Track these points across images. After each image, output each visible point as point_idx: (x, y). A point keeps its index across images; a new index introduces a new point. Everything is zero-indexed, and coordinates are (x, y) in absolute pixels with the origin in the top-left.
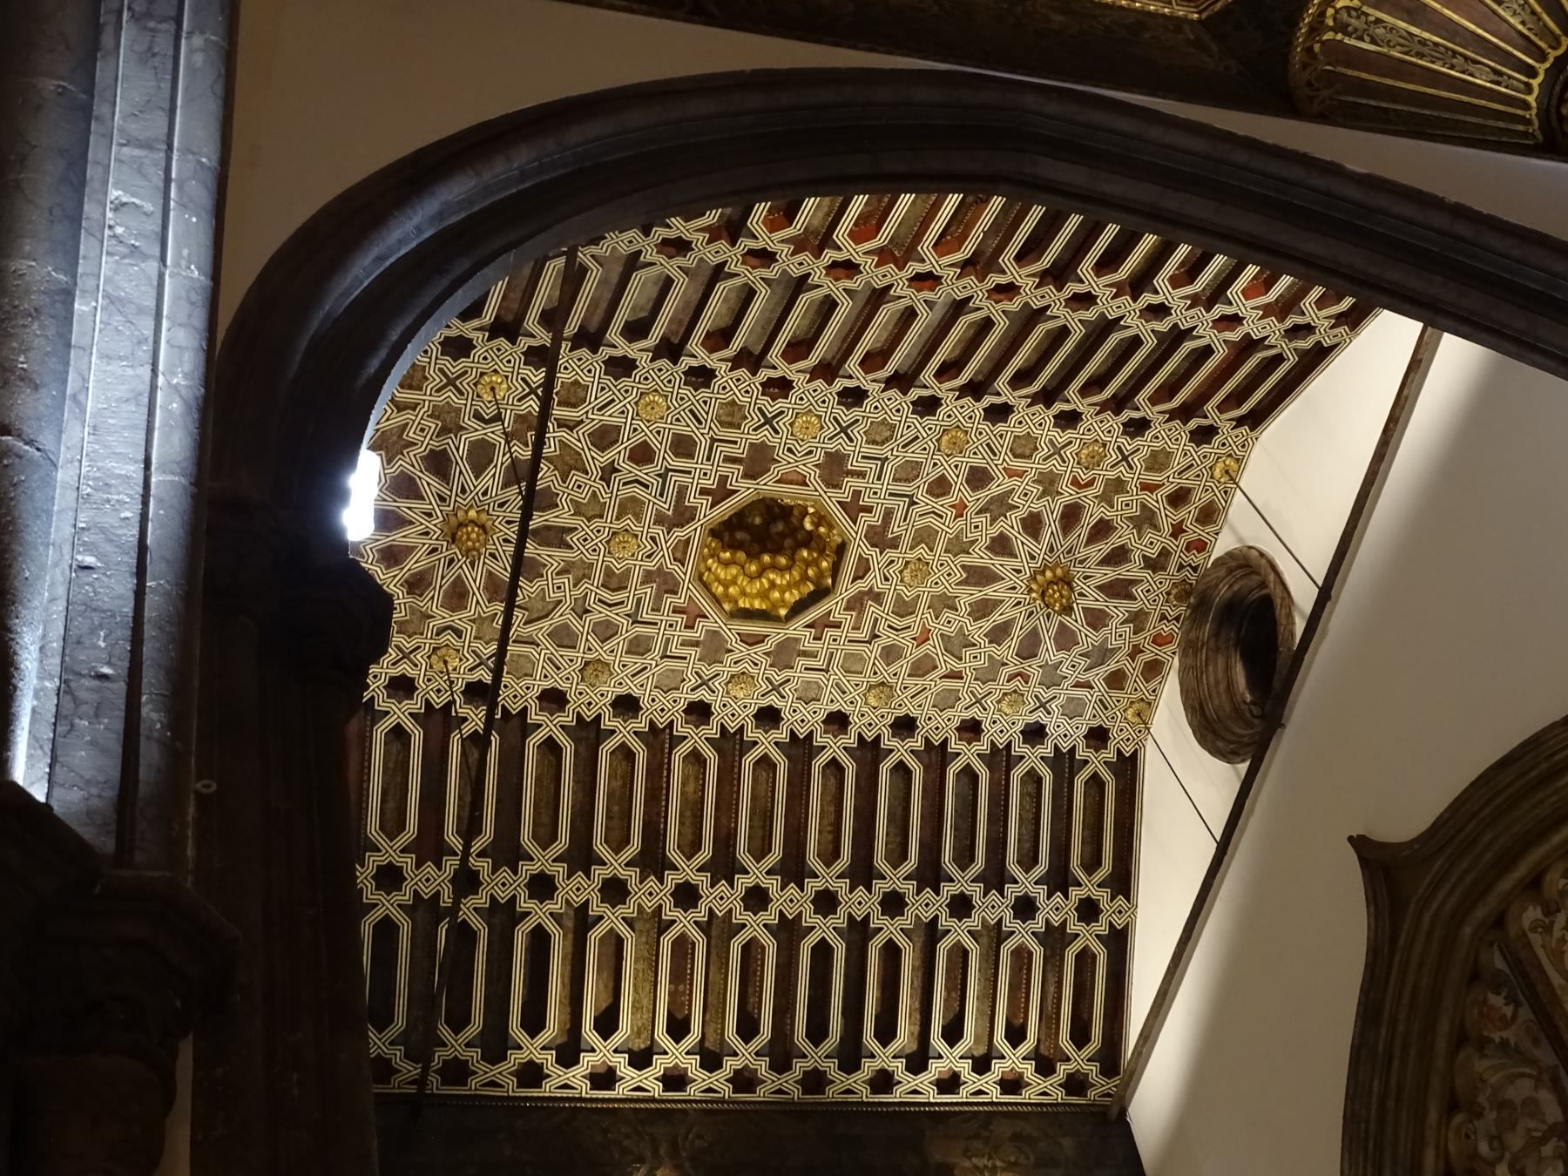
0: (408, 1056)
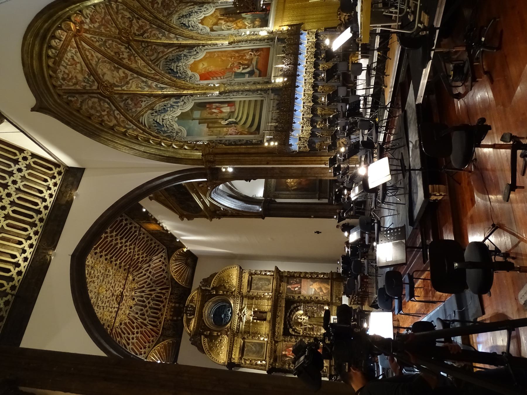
0: (6, 297)
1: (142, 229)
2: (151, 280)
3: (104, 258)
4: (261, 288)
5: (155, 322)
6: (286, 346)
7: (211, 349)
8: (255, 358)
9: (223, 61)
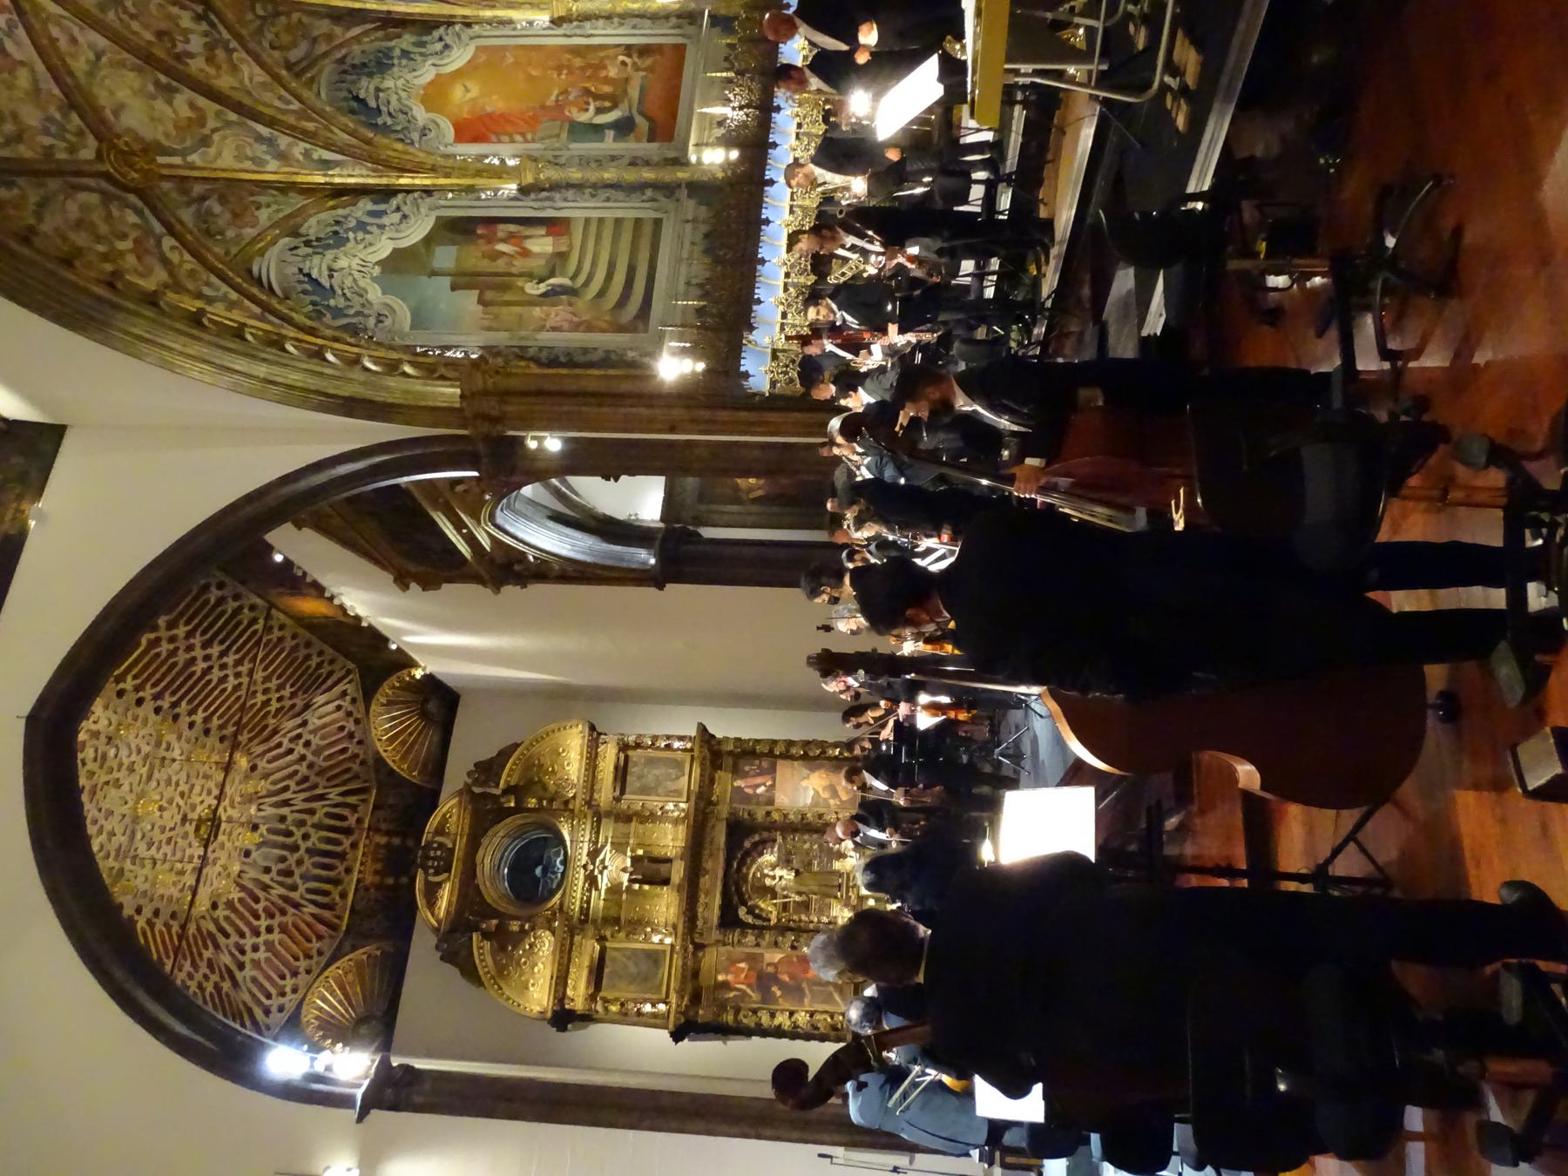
1: (274, 612)
2: (311, 766)
3: (149, 706)
4: (656, 788)
5: (326, 893)
6: (729, 958)
7: (501, 971)
9: (530, 78)
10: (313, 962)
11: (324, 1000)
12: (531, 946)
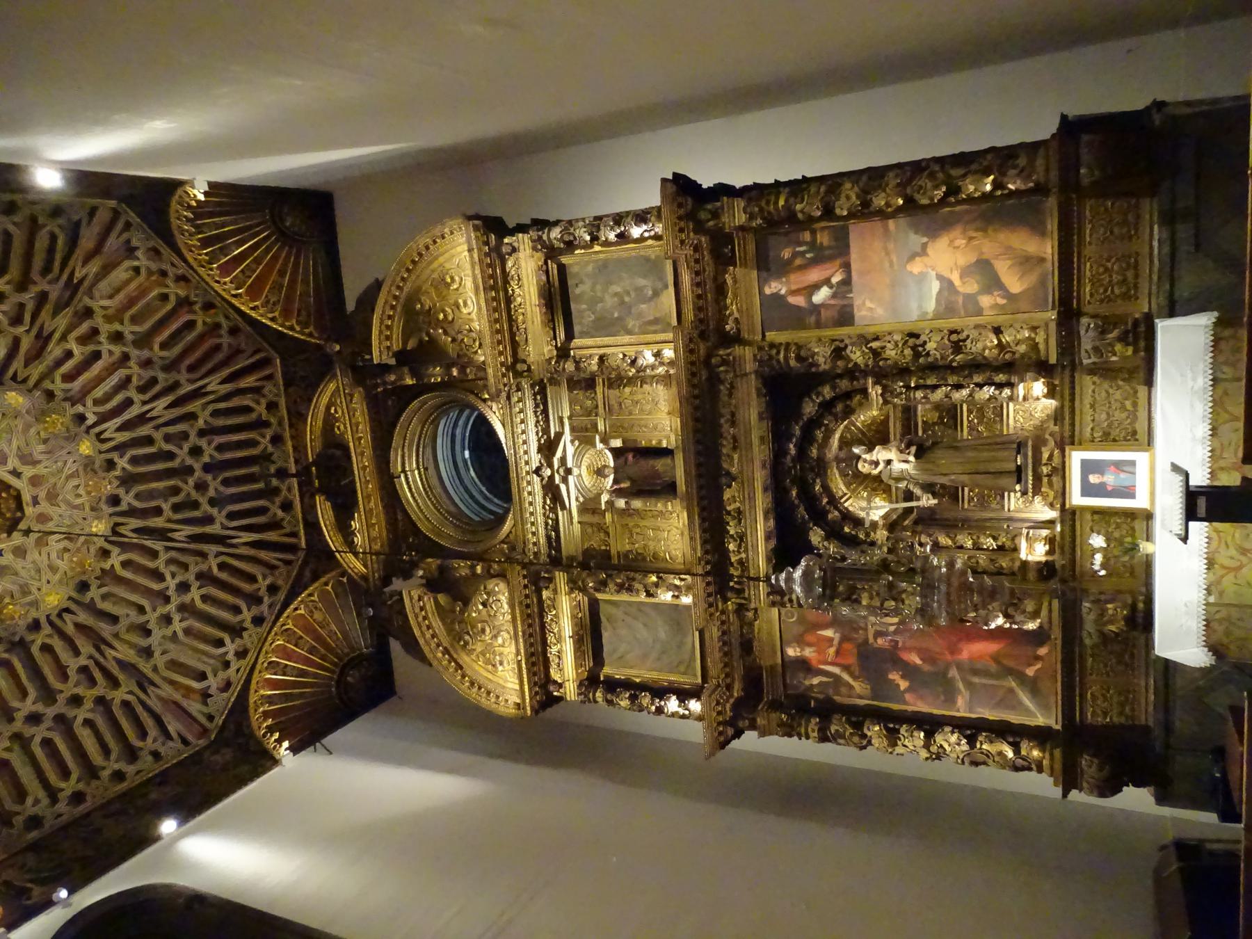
5: (262, 511)
7: (457, 637)
8: (654, 675)
10: (264, 608)
11: (289, 655)
12: (484, 604)
